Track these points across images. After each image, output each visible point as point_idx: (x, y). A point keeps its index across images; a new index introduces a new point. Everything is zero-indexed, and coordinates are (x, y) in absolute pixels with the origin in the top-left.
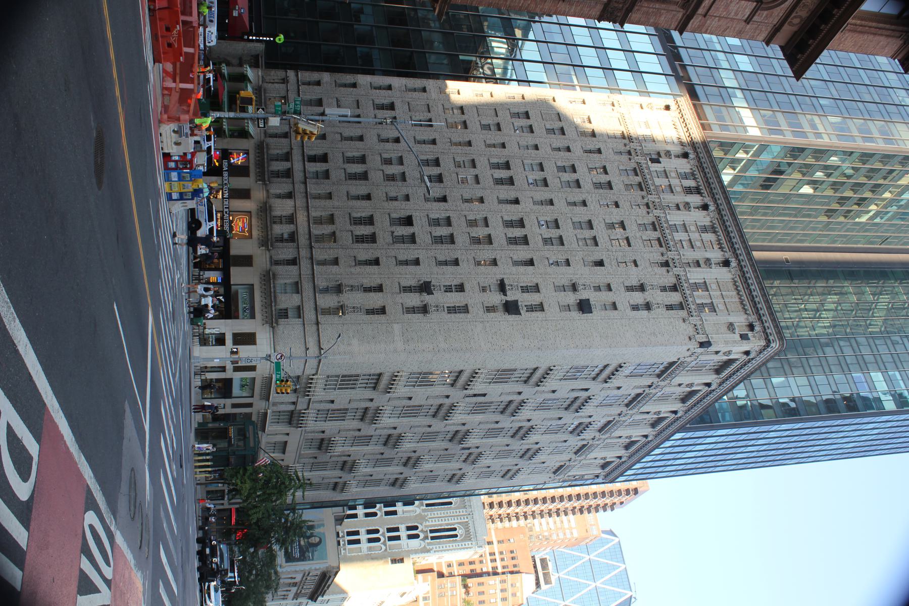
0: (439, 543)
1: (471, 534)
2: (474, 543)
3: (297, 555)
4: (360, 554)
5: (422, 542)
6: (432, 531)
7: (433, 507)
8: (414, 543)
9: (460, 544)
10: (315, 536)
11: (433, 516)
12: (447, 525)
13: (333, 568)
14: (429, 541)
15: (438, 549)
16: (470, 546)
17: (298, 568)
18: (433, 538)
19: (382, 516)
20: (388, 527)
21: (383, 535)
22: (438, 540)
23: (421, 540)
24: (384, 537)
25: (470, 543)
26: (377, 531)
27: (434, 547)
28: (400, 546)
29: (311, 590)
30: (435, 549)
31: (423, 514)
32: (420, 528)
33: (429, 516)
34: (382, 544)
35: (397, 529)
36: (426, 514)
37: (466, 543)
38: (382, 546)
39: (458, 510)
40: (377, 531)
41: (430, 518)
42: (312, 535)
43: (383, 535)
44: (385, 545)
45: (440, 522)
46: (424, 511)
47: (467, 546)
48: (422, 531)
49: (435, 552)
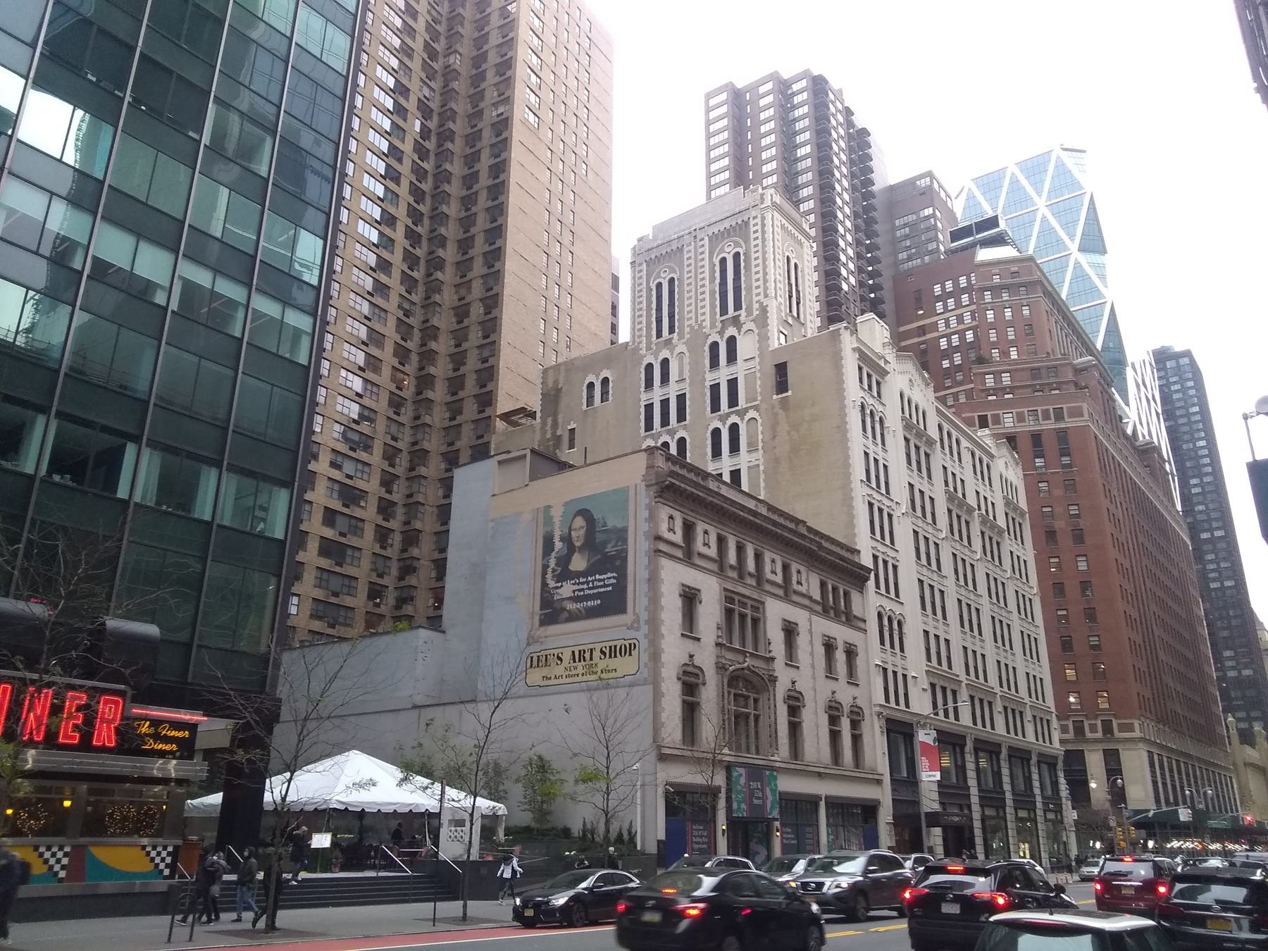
0: (749, 290)
1: (734, 224)
2: (753, 213)
3: (610, 577)
4: (762, 468)
5: (745, 328)
6: (724, 310)
7: (677, 317)
8: (746, 347)
9: (753, 243)
10: (570, 530)
11: (693, 315)
12: (712, 279)
13: (650, 467)
14: (743, 313)
15: (761, 290)
16: (758, 220)
17: (643, 574)
18: (738, 307)
19: (685, 427)
20: (709, 409)
21: (723, 419)
22: (743, 293)
23: (739, 332)
24: (728, 415)
25: (752, 222)
26: (716, 433)
27: (755, 299)
28: (750, 377)
29: (802, 569)
30: (761, 297)
31: (687, 336)
32: (714, 337)
33: (693, 322)
34: (742, 419)
35: (715, 388)
36: (687, 330)
37: (753, 229)
38: (747, 417)
39: (686, 263)
40: (716, 433)
41: (697, 318)
42: (567, 539)
43: (723, 419)
44: (746, 410)
45: (707, 296)
46: (681, 336)
47: (759, 227)
48: (721, 333)
49: (766, 296)
